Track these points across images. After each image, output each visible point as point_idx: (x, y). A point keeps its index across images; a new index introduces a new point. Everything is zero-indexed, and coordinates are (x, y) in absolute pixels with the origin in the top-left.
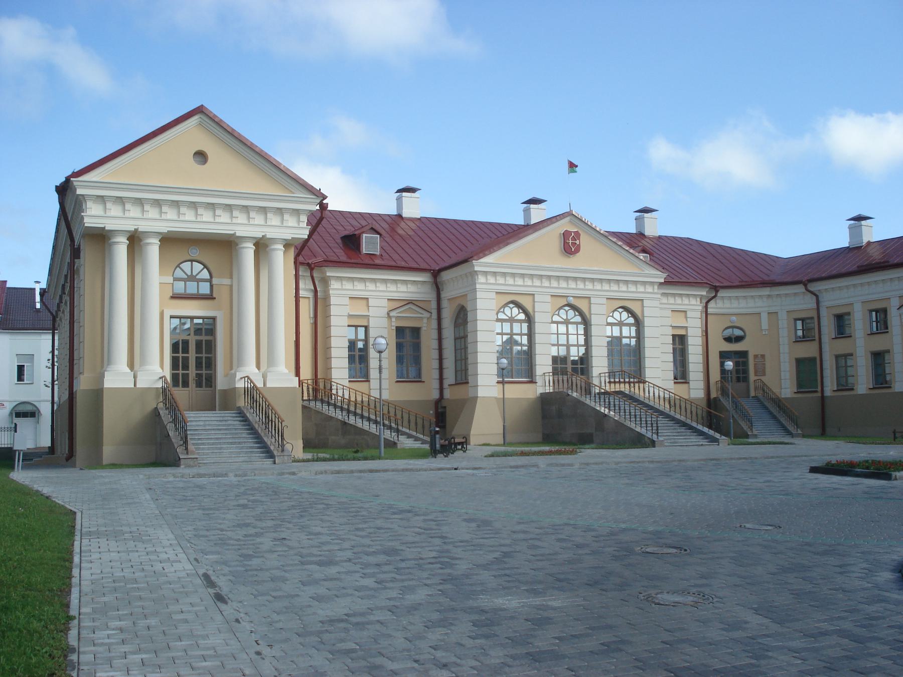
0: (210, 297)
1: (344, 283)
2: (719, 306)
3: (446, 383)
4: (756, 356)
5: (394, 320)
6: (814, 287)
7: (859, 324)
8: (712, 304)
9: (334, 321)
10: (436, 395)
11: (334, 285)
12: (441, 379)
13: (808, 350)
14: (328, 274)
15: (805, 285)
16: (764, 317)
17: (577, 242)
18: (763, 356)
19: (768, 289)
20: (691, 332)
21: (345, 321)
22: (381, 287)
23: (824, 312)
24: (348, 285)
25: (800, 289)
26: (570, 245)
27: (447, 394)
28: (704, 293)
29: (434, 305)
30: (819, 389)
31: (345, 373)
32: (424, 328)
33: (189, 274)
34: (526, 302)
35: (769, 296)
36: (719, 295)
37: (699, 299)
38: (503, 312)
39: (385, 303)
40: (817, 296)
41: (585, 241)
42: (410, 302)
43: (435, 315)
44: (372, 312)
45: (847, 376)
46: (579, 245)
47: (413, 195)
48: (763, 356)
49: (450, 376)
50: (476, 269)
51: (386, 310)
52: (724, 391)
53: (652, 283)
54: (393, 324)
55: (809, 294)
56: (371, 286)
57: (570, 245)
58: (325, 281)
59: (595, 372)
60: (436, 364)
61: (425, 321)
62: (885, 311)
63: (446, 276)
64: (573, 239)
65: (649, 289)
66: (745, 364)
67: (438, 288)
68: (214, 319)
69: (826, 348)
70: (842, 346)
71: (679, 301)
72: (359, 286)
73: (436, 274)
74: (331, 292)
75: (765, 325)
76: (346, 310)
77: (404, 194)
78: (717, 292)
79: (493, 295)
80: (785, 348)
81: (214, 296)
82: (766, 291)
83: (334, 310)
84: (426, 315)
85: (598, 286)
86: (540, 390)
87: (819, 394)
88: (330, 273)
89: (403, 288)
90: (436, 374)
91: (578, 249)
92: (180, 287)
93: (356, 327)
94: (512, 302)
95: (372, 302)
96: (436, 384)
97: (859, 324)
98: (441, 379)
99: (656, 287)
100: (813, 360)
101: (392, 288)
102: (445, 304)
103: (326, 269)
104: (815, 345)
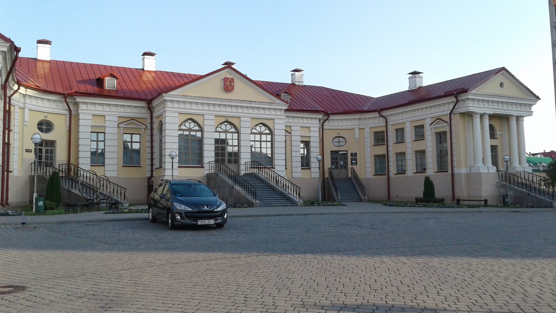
1: (89, 106)
2: (330, 124)
3: (154, 167)
4: (352, 154)
5: (122, 129)
6: (385, 113)
7: (409, 134)
8: (326, 123)
9: (81, 129)
10: (149, 174)
11: (82, 107)
12: (152, 165)
13: (381, 150)
14: (77, 100)
15: (379, 112)
16: (357, 130)
17: (232, 84)
18: (356, 154)
19: (359, 115)
20: (312, 140)
21: (89, 129)
22: (114, 109)
23: (389, 127)
24: (92, 107)
25: (376, 114)
26: (228, 86)
27: (154, 175)
28: (321, 117)
29: (149, 121)
31: (89, 161)
34: (199, 119)
35: (360, 119)
36: (330, 118)
37: (318, 120)
38: (185, 125)
39: (116, 119)
41: (238, 84)
42: (133, 119)
44: (107, 124)
45: (402, 166)
47: (151, 57)
48: (356, 154)
49: (156, 164)
50: (165, 98)
51: (117, 123)
52: (331, 173)
53: (280, 110)
54: (122, 132)
55: (382, 118)
56: (107, 108)
57: (228, 86)
58: (77, 104)
59: (242, 161)
60: (149, 156)
61: (143, 130)
62: (422, 126)
63: (155, 103)
65: (279, 113)
67: (151, 109)
69: (391, 148)
70: (400, 148)
71: (305, 121)
72: (99, 108)
73: (149, 102)
74: (80, 111)
75: (357, 136)
76: (91, 123)
77: (145, 56)
78: (329, 116)
79: (177, 115)
80: (368, 149)
82: (358, 116)
83: (81, 122)
84: (145, 127)
85: (245, 111)
86: (207, 172)
87: (386, 176)
88: (79, 99)
89: (129, 110)
90: (149, 162)
91: (233, 88)
93: (98, 133)
94: (190, 119)
95: (107, 118)
96: (149, 168)
97: (409, 134)
98: (152, 165)
99: (283, 112)
100: (383, 156)
101: (122, 110)
102: (155, 120)
103: (76, 97)
104: (385, 147)
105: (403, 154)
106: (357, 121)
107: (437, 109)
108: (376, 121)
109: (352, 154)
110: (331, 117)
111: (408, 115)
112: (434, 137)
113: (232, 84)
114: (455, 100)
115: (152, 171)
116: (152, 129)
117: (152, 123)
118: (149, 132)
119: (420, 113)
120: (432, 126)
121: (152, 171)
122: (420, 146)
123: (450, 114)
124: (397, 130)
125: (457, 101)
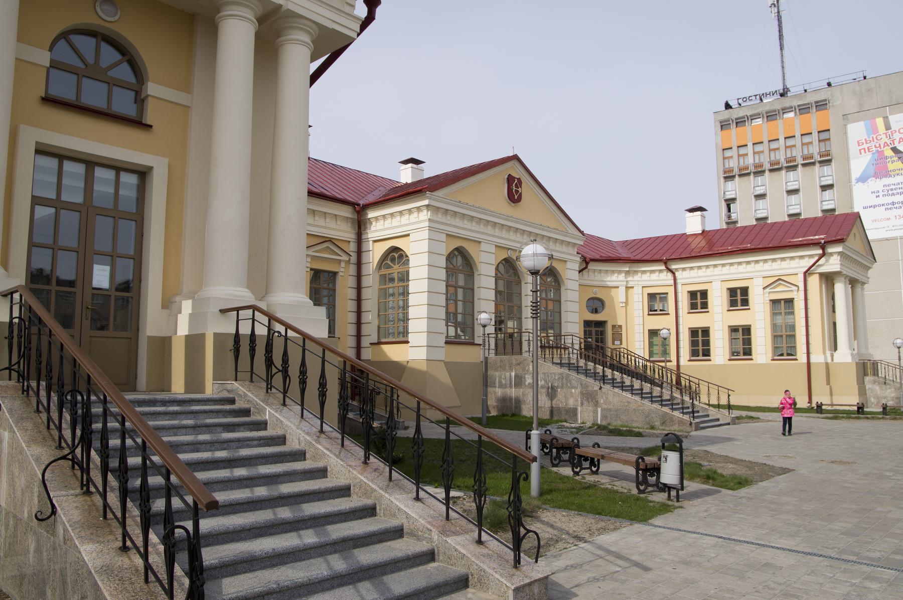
0: (138, 123)
3: (365, 342)
4: (614, 326)
7: (718, 299)
12: (359, 336)
15: (665, 263)
16: (622, 290)
17: (519, 189)
19: (629, 265)
29: (352, 247)
30: (673, 357)
32: (341, 274)
33: (91, 60)
40: (674, 273)
41: (527, 190)
42: (330, 240)
43: (354, 259)
46: (521, 194)
60: (352, 318)
64: (516, 186)
66: (603, 333)
67: (360, 226)
68: (143, 174)
70: (698, 320)
78: (587, 263)
79: (443, 237)
81: (149, 119)
84: (344, 257)
91: (519, 199)
92: (65, 88)
97: (718, 299)
98: (359, 336)
102: (369, 245)
105: (706, 332)
106: (623, 275)
107: (776, 265)
108: (654, 276)
109: (614, 326)
110: (592, 266)
111: (717, 271)
112: (768, 306)
113: (519, 189)
114: (820, 252)
115: (358, 348)
116: (359, 264)
117: (359, 252)
118: (352, 270)
119: (742, 268)
120: (768, 290)
121: (358, 348)
122: (740, 318)
123: (805, 273)
124: (693, 295)
125: (823, 255)
